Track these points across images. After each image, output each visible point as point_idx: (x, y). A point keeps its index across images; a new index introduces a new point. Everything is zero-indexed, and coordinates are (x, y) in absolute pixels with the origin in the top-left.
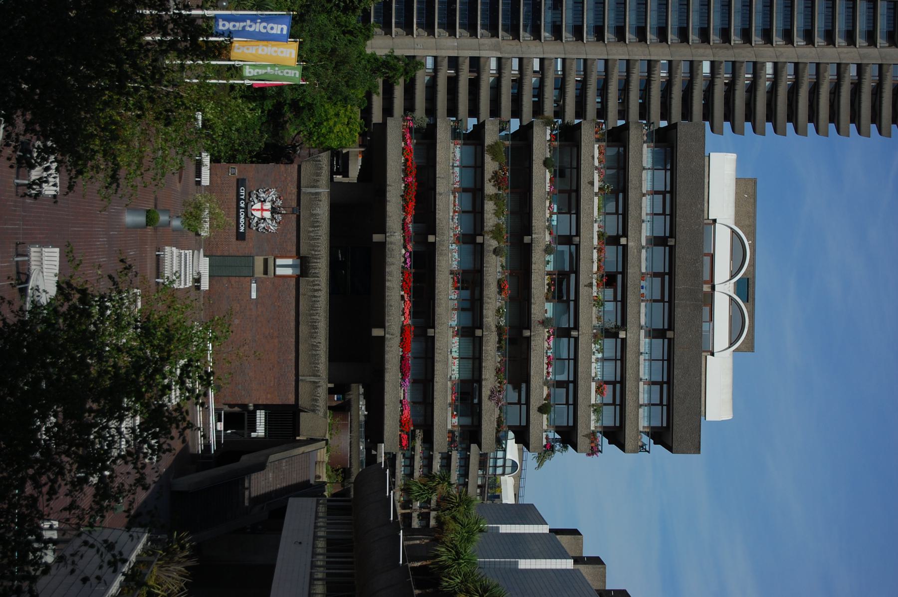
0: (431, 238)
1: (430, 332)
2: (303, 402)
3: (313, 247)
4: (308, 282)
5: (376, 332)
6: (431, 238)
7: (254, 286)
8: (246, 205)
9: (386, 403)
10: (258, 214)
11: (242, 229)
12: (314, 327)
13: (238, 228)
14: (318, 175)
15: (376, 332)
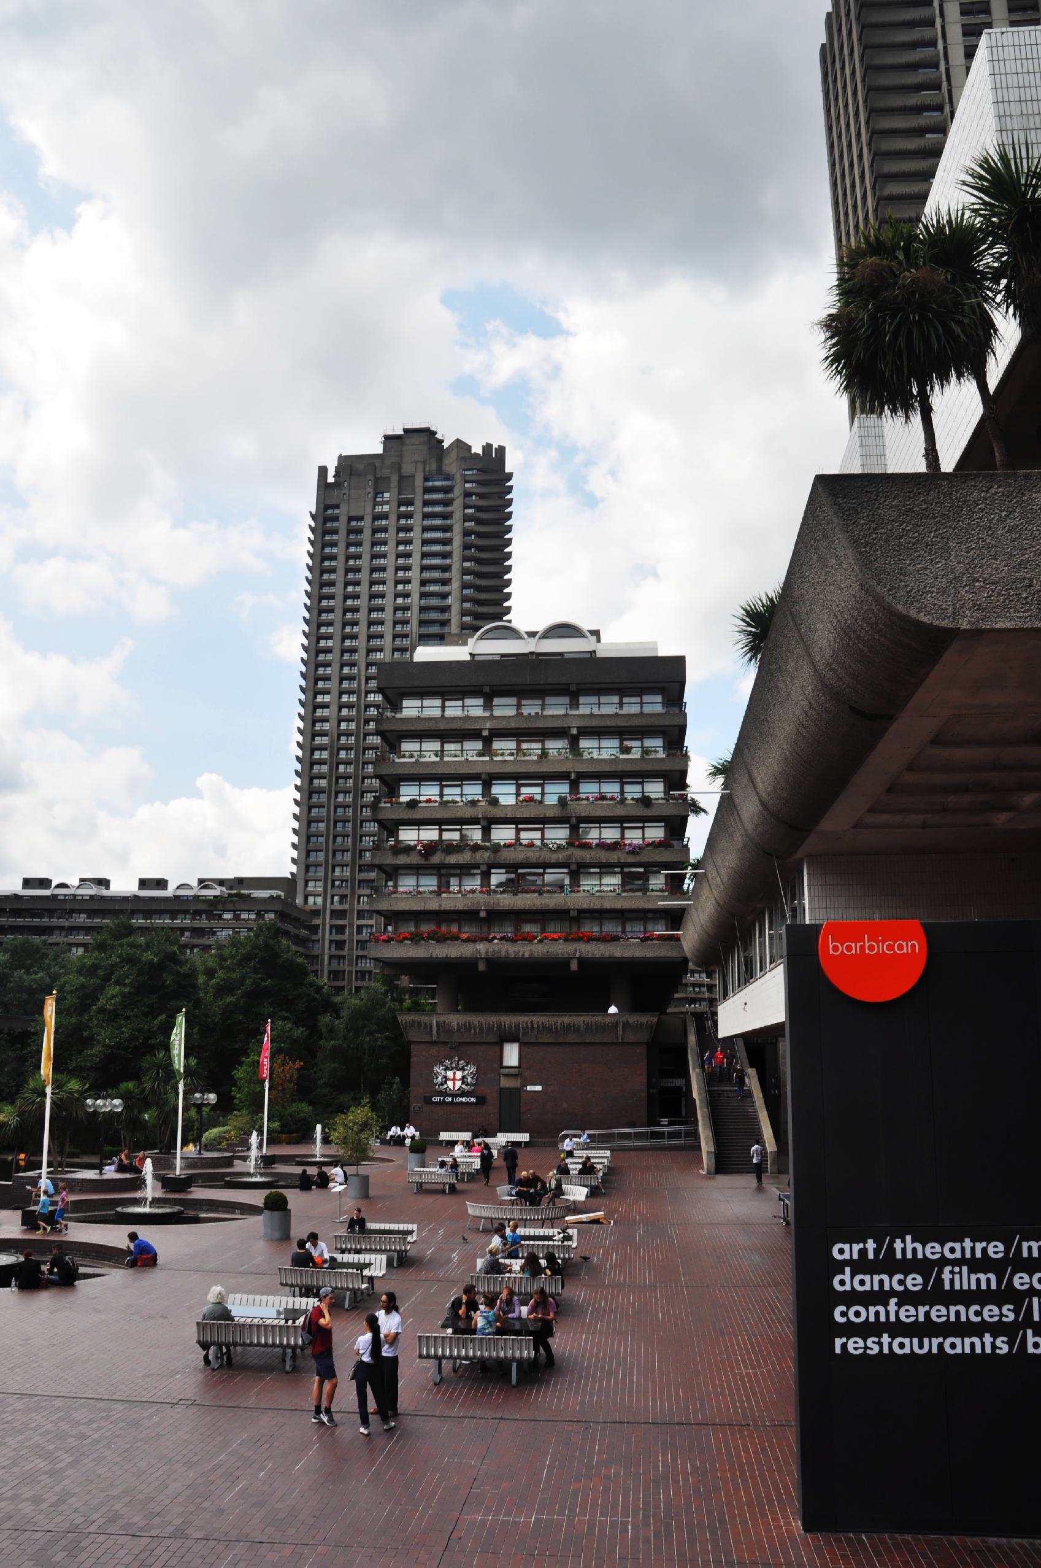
0: (483, 914)
1: (573, 914)
2: (644, 1037)
3: (490, 1029)
4: (524, 1034)
5: (574, 966)
6: (483, 914)
7: (529, 1088)
8: (450, 1095)
9: (642, 955)
10: (458, 1084)
11: (473, 1100)
12: (568, 1028)
13: (472, 1103)
14: (419, 1023)
15: (574, 966)
